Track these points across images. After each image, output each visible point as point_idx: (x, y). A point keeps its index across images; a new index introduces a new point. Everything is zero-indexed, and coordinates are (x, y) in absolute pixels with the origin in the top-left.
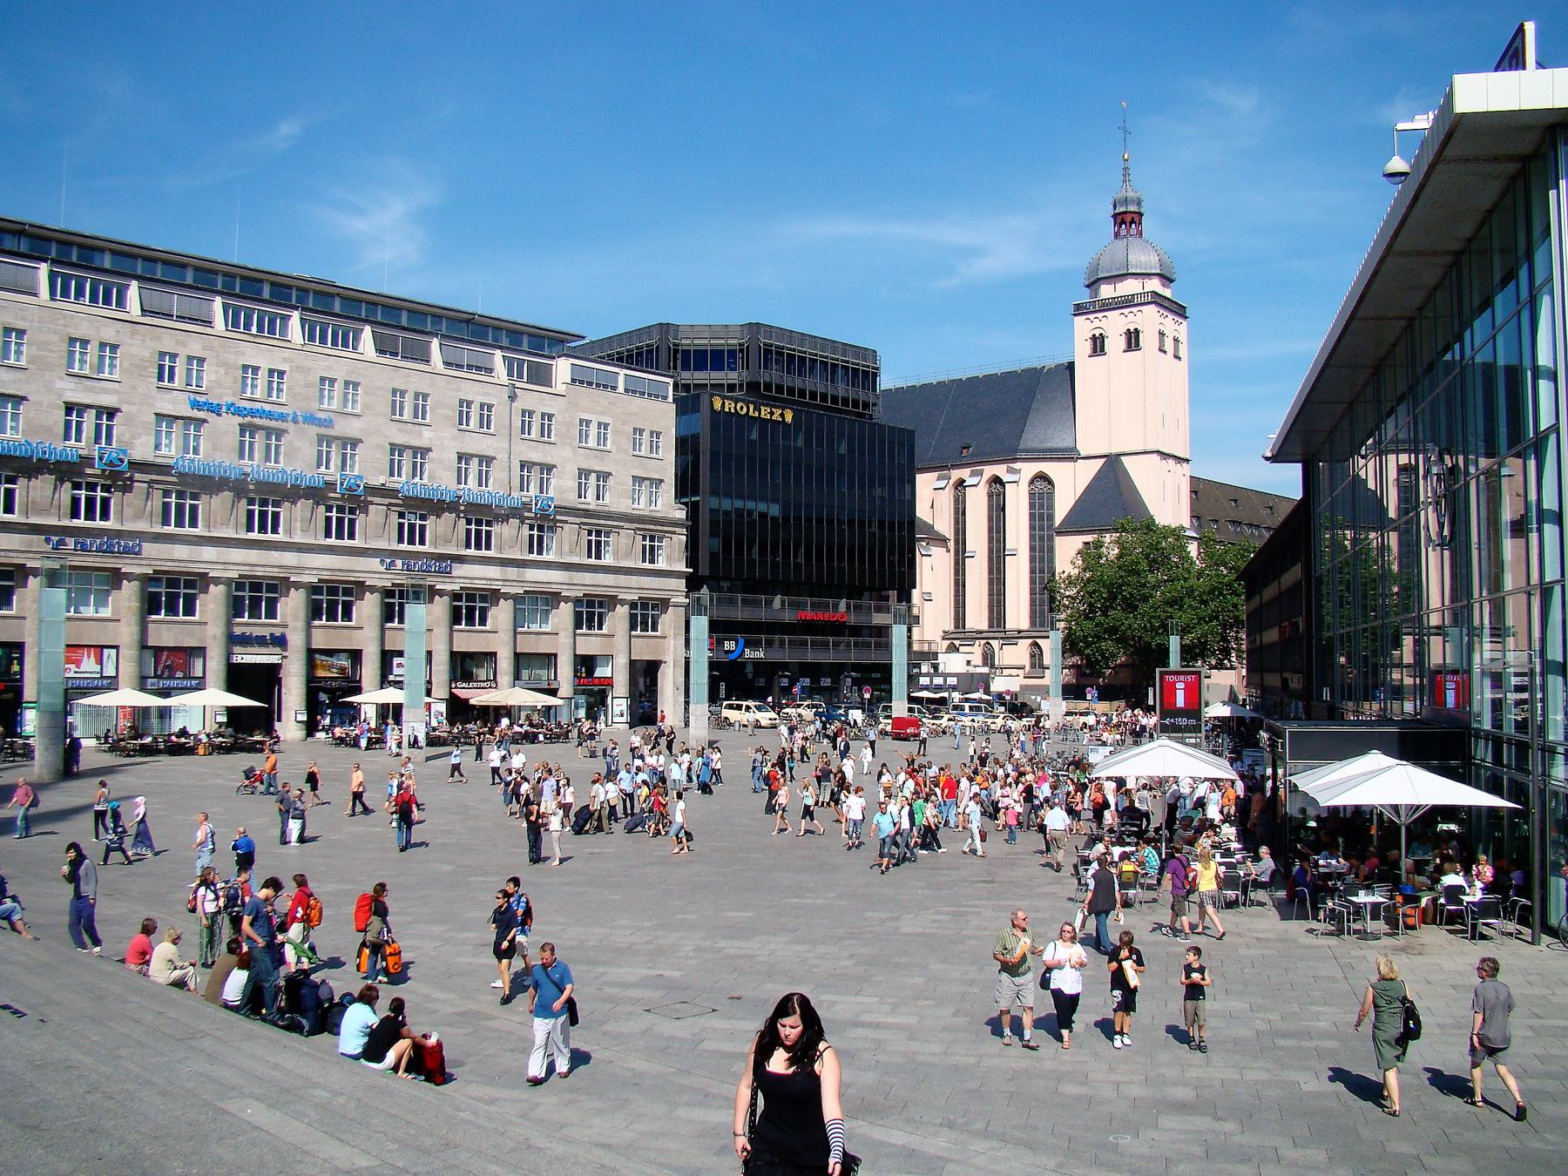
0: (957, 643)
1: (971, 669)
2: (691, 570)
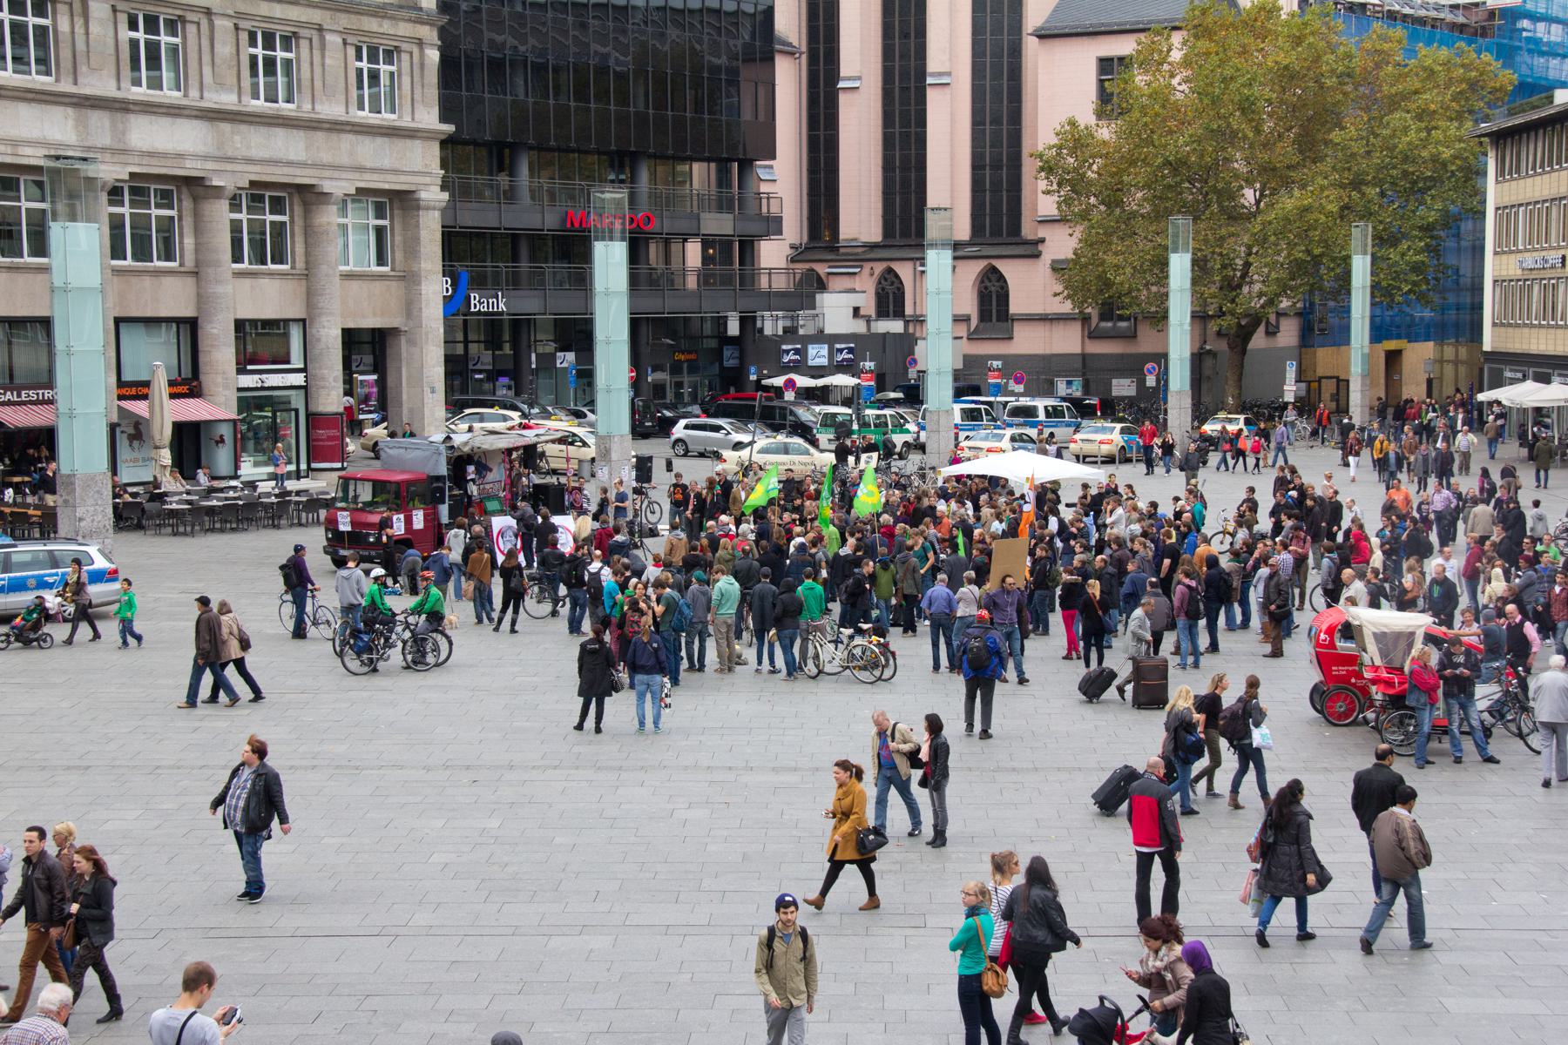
0: (822, 269)
1: (859, 327)
2: (450, 128)
